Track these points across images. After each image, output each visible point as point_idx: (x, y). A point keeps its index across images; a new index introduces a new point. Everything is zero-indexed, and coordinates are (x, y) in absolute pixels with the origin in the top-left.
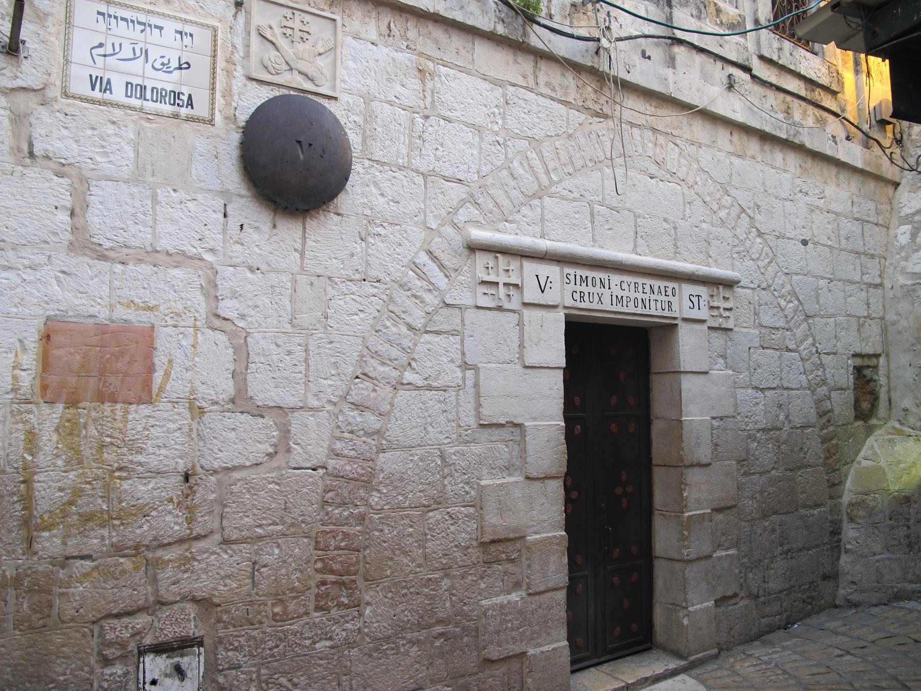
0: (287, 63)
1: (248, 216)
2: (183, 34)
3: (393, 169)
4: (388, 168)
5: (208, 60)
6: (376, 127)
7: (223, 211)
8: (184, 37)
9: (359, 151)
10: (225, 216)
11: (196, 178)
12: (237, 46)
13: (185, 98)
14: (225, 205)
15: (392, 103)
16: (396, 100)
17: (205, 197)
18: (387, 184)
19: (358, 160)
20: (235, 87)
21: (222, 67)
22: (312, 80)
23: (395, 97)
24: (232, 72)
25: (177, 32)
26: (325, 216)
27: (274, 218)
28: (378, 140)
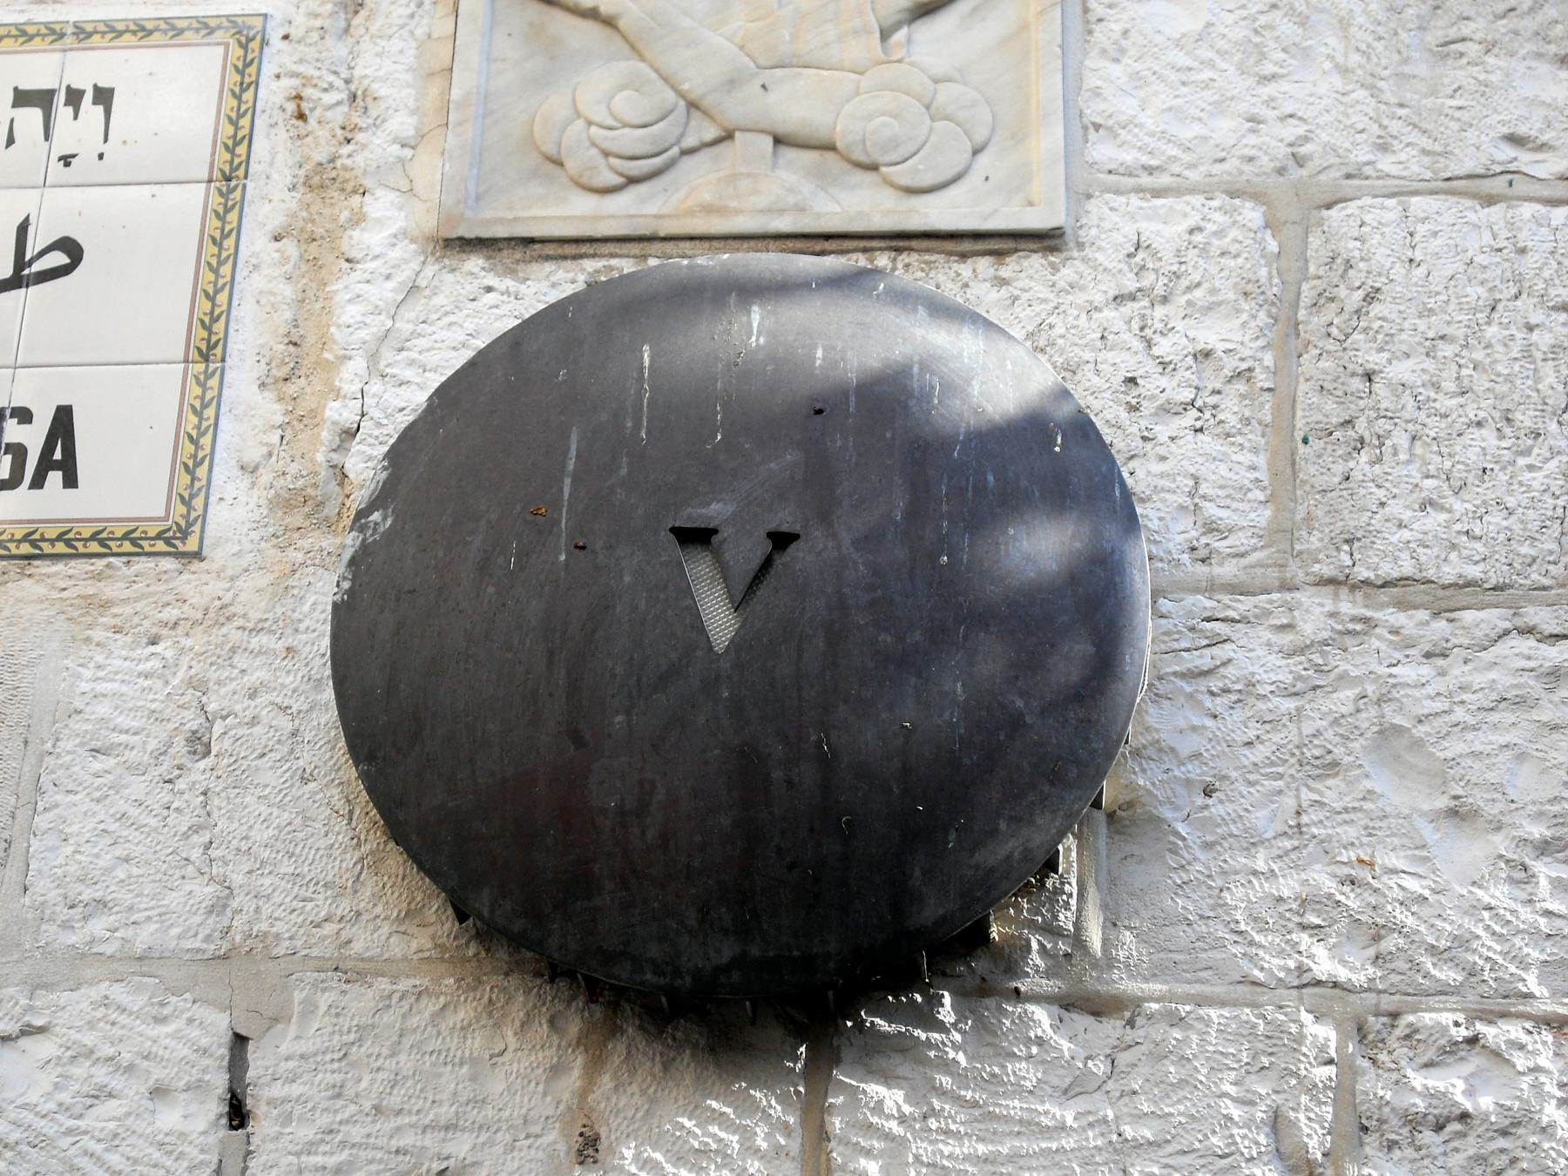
0: (693, 105)
1: (395, 1100)
2: (61, 97)
3: (1538, 615)
4: (1493, 618)
5: (192, 200)
6: (1374, 359)
7: (220, 1081)
8: (63, 112)
9: (1240, 540)
10: (237, 1114)
11: (53, 895)
12: (381, 90)
13: (33, 437)
14: (240, 1041)
15: (1498, 185)
16: (1524, 159)
17: (105, 1002)
18: (1512, 729)
19: (1245, 604)
20: (352, 313)
21: (277, 221)
22: (873, 167)
23: (1515, 140)
24: (332, 238)
25: (22, 98)
26: (985, 1035)
27: (583, 1094)
28: (1400, 438)
